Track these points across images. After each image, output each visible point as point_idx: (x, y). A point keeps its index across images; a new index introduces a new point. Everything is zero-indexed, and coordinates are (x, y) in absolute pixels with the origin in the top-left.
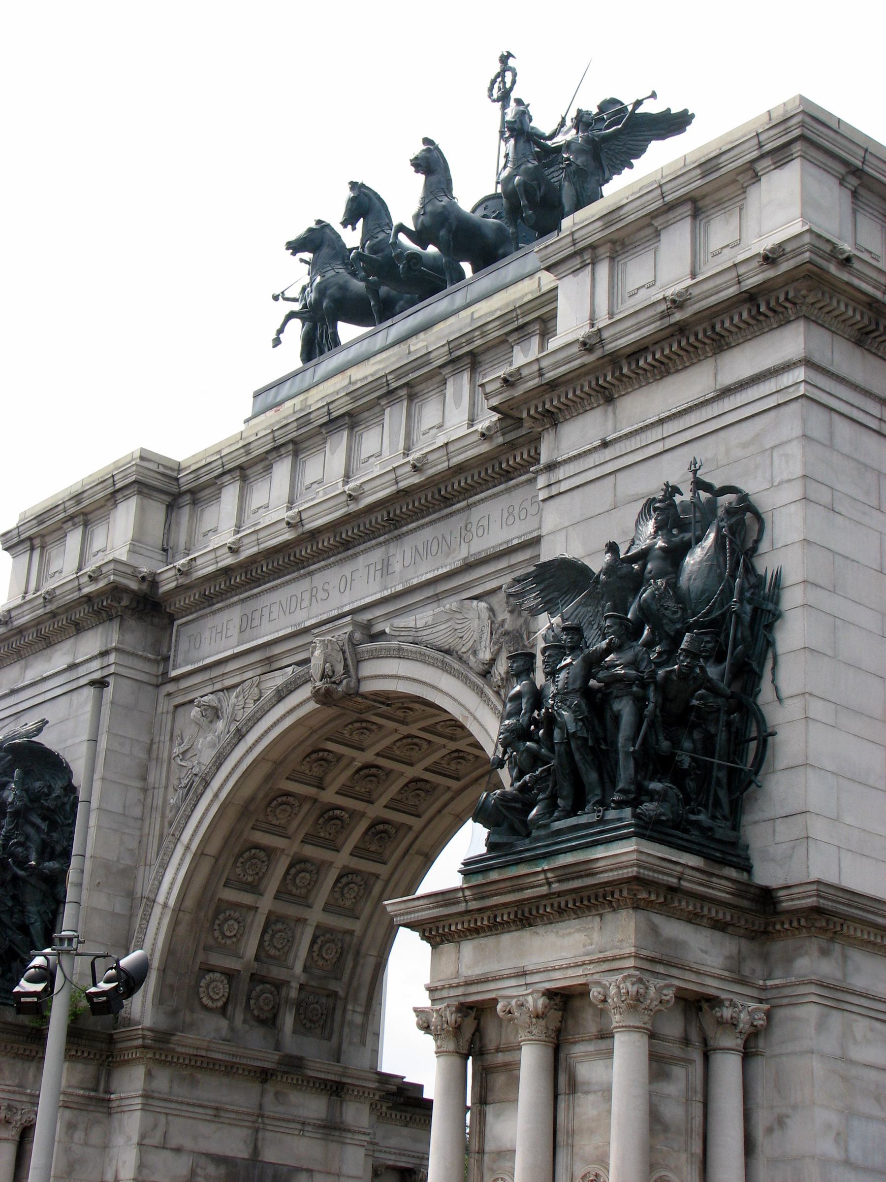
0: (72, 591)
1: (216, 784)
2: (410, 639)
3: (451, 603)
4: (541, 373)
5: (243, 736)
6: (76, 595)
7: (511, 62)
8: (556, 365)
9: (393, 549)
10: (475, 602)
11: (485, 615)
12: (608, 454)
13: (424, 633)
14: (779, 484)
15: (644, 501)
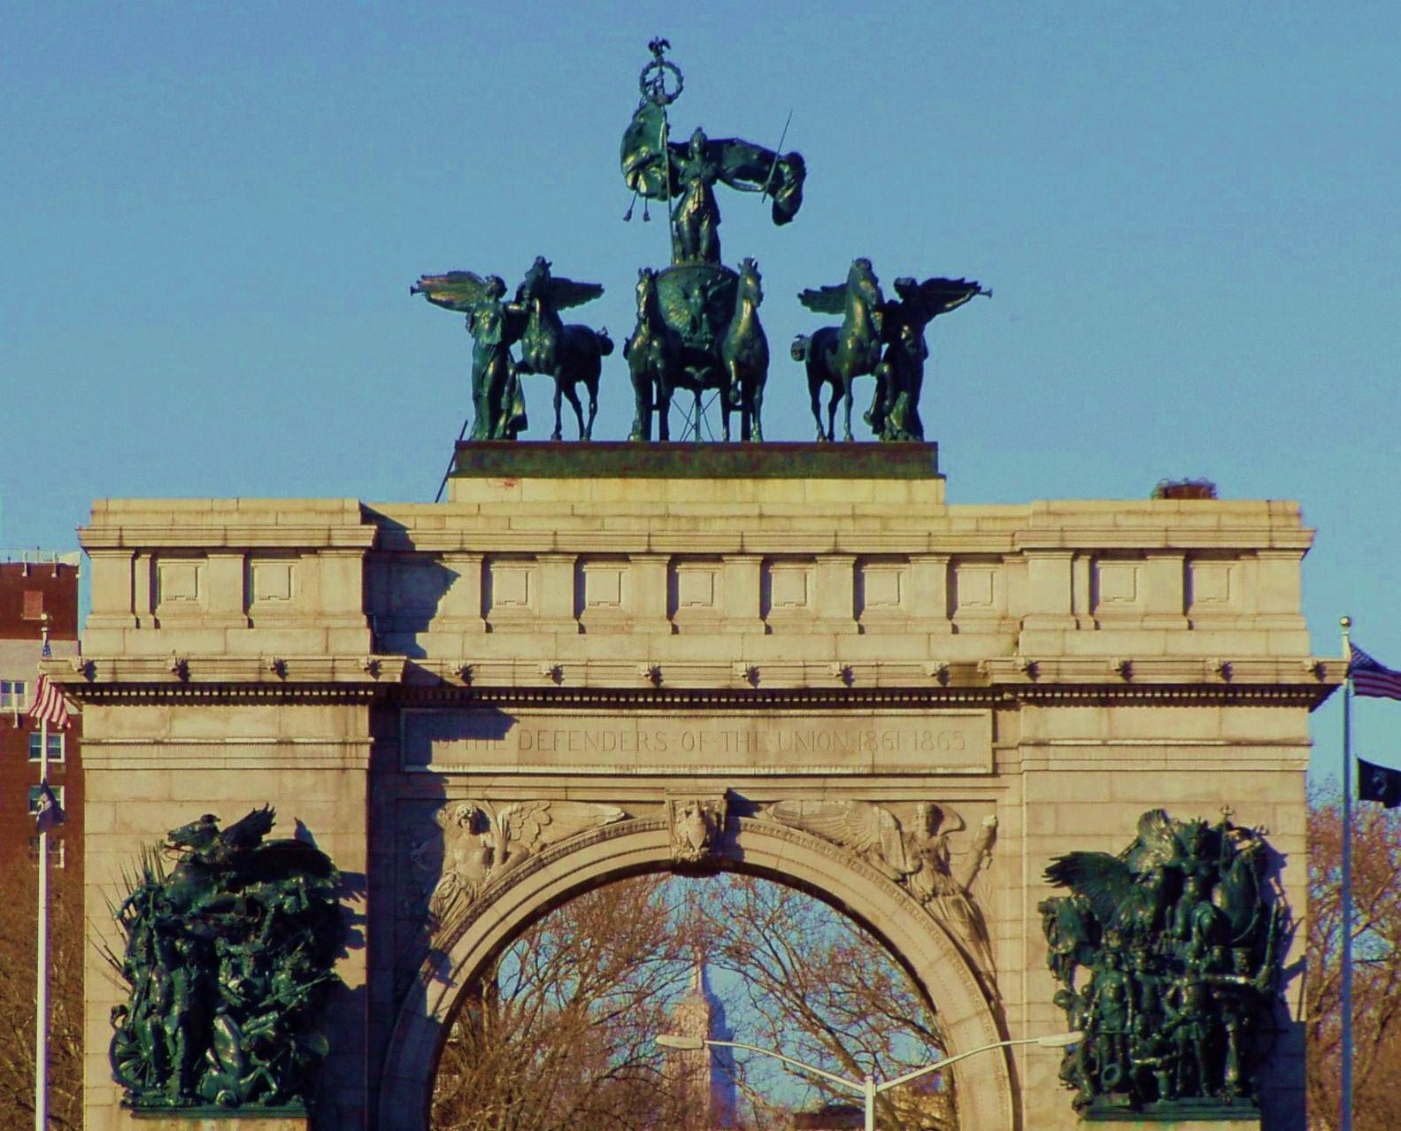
0: (321, 671)
1: (502, 906)
2: (796, 823)
3: (842, 800)
4: (1058, 672)
5: (544, 866)
6: (326, 678)
7: (668, 55)
8: (1078, 672)
9: (762, 724)
10: (876, 809)
11: (890, 823)
12: (1105, 752)
13: (813, 820)
14: (1283, 834)
15: (1149, 809)
